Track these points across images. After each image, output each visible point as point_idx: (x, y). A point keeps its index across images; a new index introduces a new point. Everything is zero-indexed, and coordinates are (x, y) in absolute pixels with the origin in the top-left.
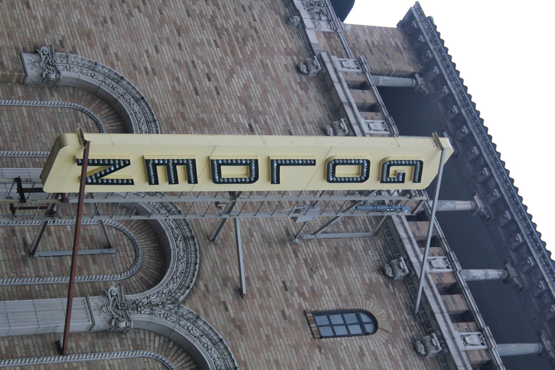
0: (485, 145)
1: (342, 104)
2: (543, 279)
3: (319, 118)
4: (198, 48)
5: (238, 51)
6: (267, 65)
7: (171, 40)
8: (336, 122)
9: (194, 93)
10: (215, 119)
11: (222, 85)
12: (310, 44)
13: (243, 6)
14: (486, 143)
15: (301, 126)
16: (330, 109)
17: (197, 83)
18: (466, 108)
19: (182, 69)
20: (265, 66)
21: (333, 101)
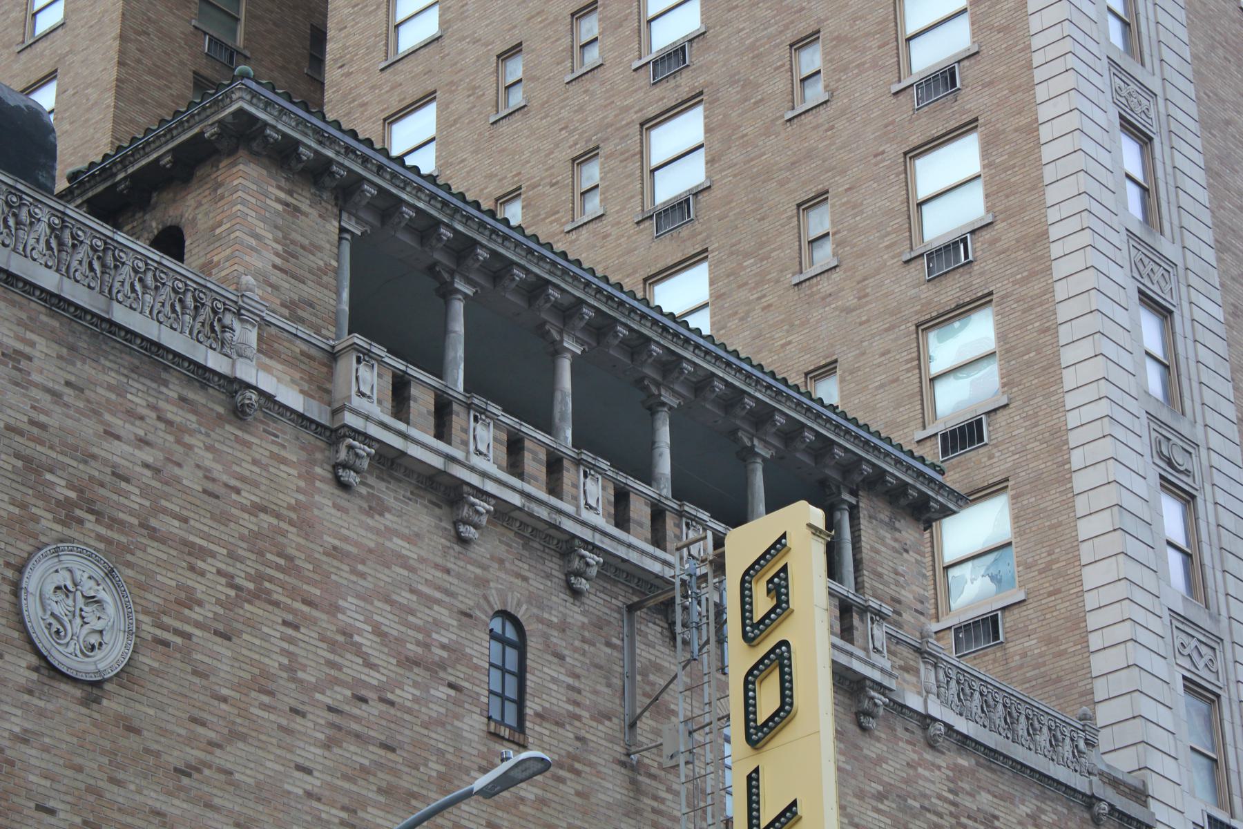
0: (524, 254)
1: (443, 473)
2: (713, 375)
3: (437, 527)
4: (300, 674)
5: (305, 587)
6: (335, 548)
7: (284, 722)
8: (466, 512)
9: (390, 755)
10: (438, 749)
11: (375, 682)
12: (302, 416)
13: (205, 491)
14: (523, 249)
15: (451, 579)
16: (418, 488)
17: (372, 733)
18: (458, 216)
19: (345, 745)
20: (335, 553)
21: (413, 471)
